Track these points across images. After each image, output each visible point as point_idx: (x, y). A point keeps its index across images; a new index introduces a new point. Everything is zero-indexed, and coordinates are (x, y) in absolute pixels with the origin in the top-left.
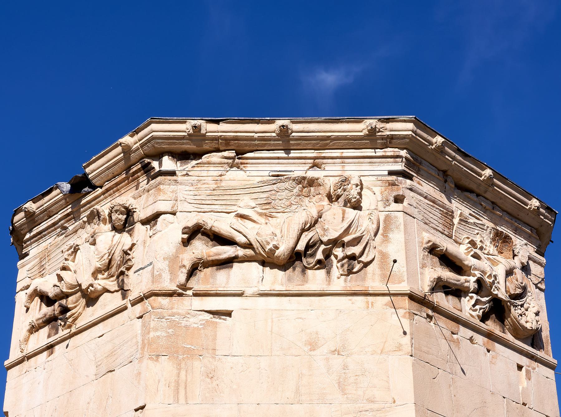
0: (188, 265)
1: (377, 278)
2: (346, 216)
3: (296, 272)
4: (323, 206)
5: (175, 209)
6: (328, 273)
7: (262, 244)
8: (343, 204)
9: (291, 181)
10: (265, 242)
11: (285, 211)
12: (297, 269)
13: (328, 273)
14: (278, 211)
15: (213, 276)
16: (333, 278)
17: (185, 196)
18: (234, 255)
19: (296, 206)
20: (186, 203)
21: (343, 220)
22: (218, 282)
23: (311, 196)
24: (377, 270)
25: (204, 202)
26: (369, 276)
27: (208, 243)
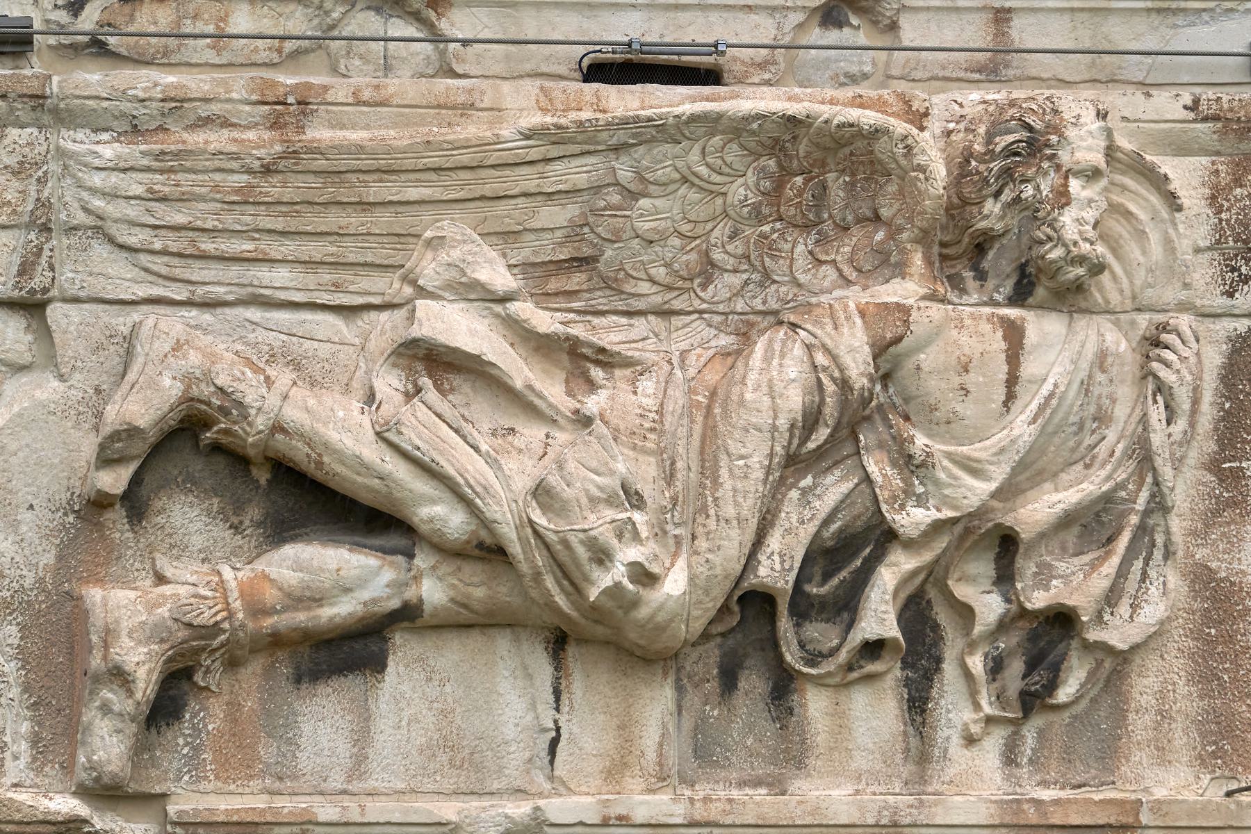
0: (143, 663)
1: (1181, 738)
2: (1029, 368)
3: (739, 698)
4: (904, 310)
5: (37, 282)
6: (918, 704)
7: (563, 556)
8: (1008, 288)
9: (717, 140)
10: (582, 552)
11: (677, 304)
12: (742, 684)
13: (918, 704)
14: (640, 305)
15: (281, 728)
16: (941, 734)
17: (98, 203)
18: (395, 604)
19: (736, 280)
20: (100, 250)
21: (1010, 397)
22: (305, 760)
23: (828, 227)
24: (1182, 689)
25: (208, 246)
26: (1140, 724)
27: (239, 509)
